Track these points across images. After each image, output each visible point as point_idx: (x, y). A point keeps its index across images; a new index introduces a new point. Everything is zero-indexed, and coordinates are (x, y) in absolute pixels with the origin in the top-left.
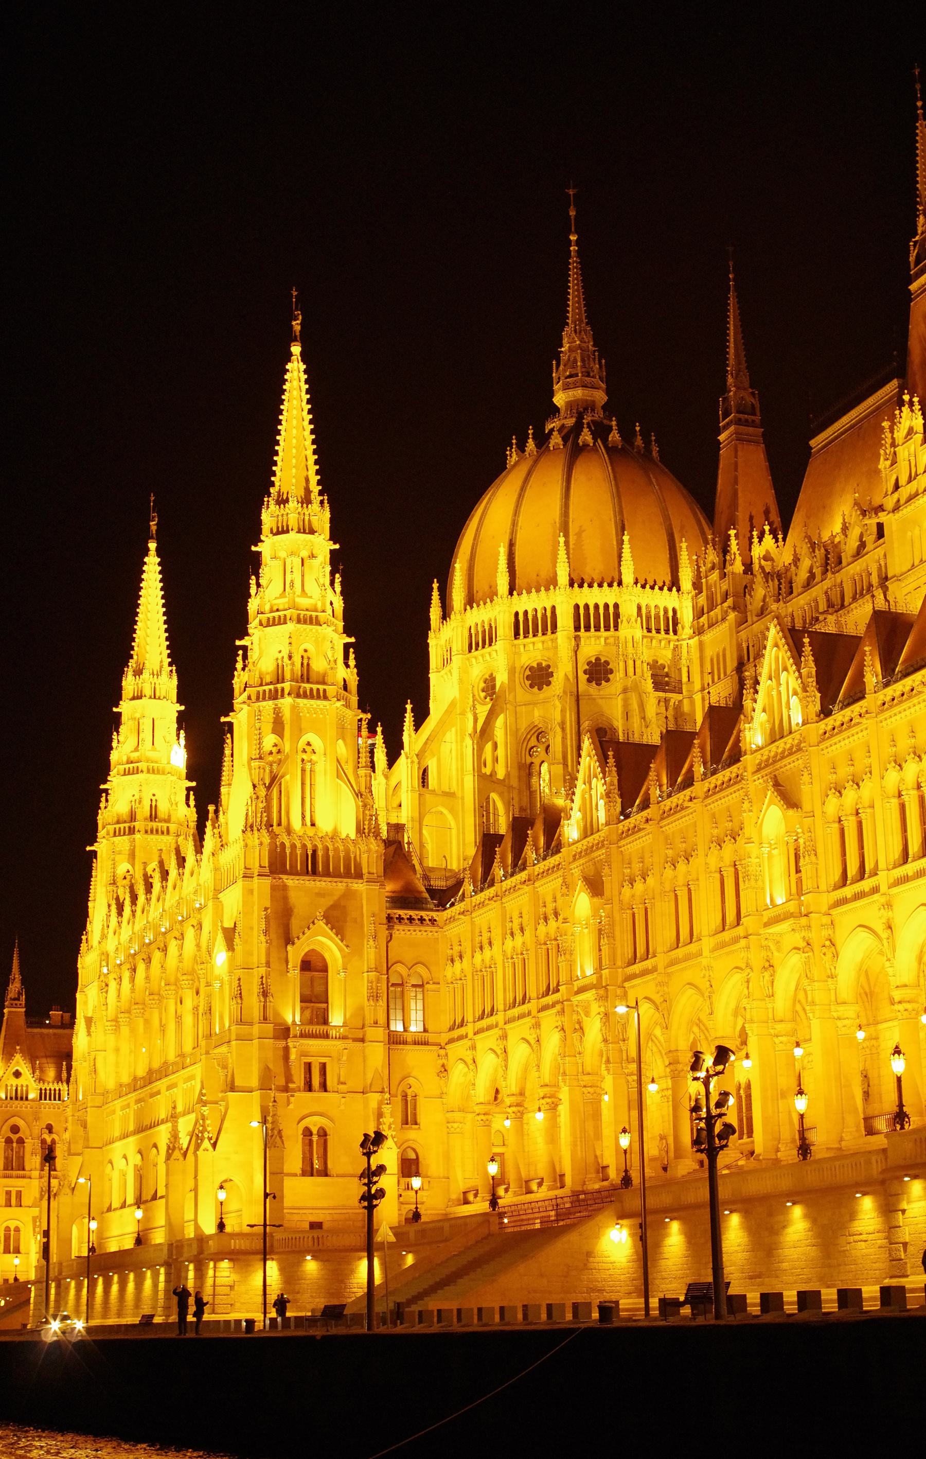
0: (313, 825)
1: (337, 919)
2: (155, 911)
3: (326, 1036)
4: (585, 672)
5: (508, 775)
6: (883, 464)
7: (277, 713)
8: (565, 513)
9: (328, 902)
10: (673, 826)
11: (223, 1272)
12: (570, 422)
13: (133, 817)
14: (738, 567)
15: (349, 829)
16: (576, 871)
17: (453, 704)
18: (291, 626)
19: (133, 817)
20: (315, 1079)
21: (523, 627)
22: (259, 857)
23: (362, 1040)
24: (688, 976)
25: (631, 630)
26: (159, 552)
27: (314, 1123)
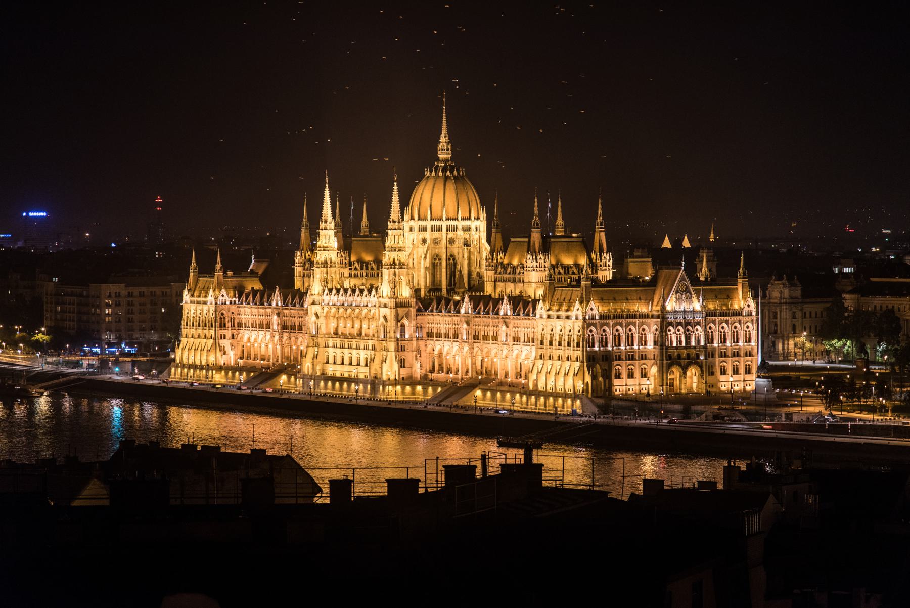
1: (407, 315)
10: (485, 320)
11: (389, 388)
19: (326, 262)
21: (435, 229)
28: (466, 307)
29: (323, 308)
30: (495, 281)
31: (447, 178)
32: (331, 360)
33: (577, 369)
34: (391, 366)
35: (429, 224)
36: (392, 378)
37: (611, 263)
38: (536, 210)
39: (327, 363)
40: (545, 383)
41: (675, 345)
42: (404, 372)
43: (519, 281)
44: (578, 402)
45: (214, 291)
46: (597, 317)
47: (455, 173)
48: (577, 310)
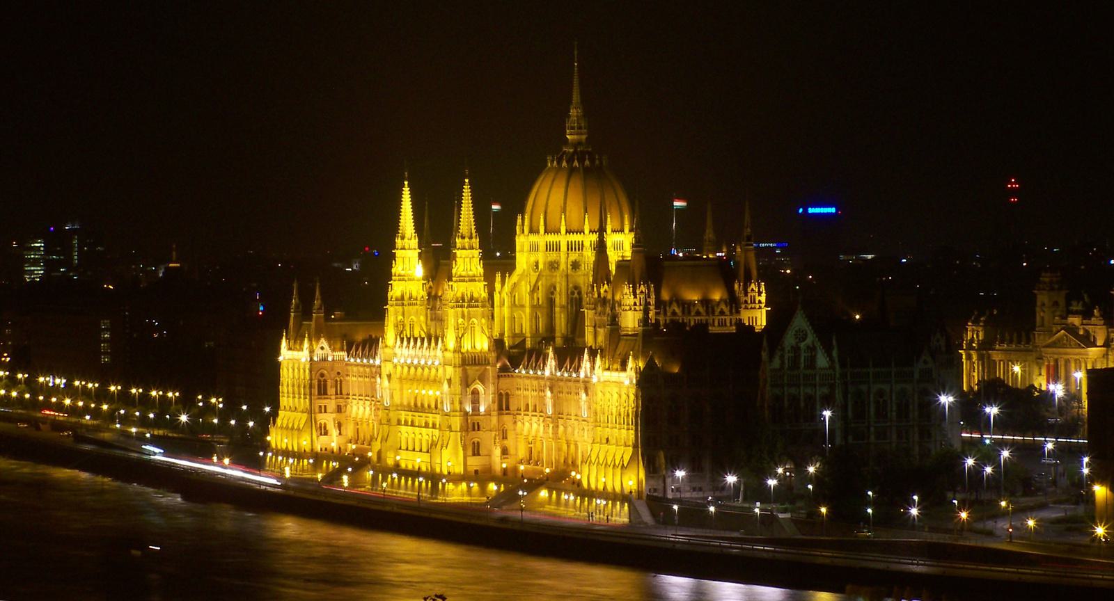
0: (474, 347)
1: (482, 379)
3: (479, 415)
4: (571, 265)
5: (543, 303)
7: (463, 312)
8: (565, 203)
9: (479, 373)
11: (450, 486)
13: (402, 298)
14: (596, 296)
15: (486, 348)
16: (548, 383)
19: (402, 298)
20: (476, 427)
22: (458, 361)
23: (490, 415)
26: (409, 186)
27: (476, 440)
29: (395, 366)
31: (572, 171)
32: (404, 447)
37: (763, 298)
39: (400, 449)
42: (475, 463)
45: (310, 340)
47: (587, 163)
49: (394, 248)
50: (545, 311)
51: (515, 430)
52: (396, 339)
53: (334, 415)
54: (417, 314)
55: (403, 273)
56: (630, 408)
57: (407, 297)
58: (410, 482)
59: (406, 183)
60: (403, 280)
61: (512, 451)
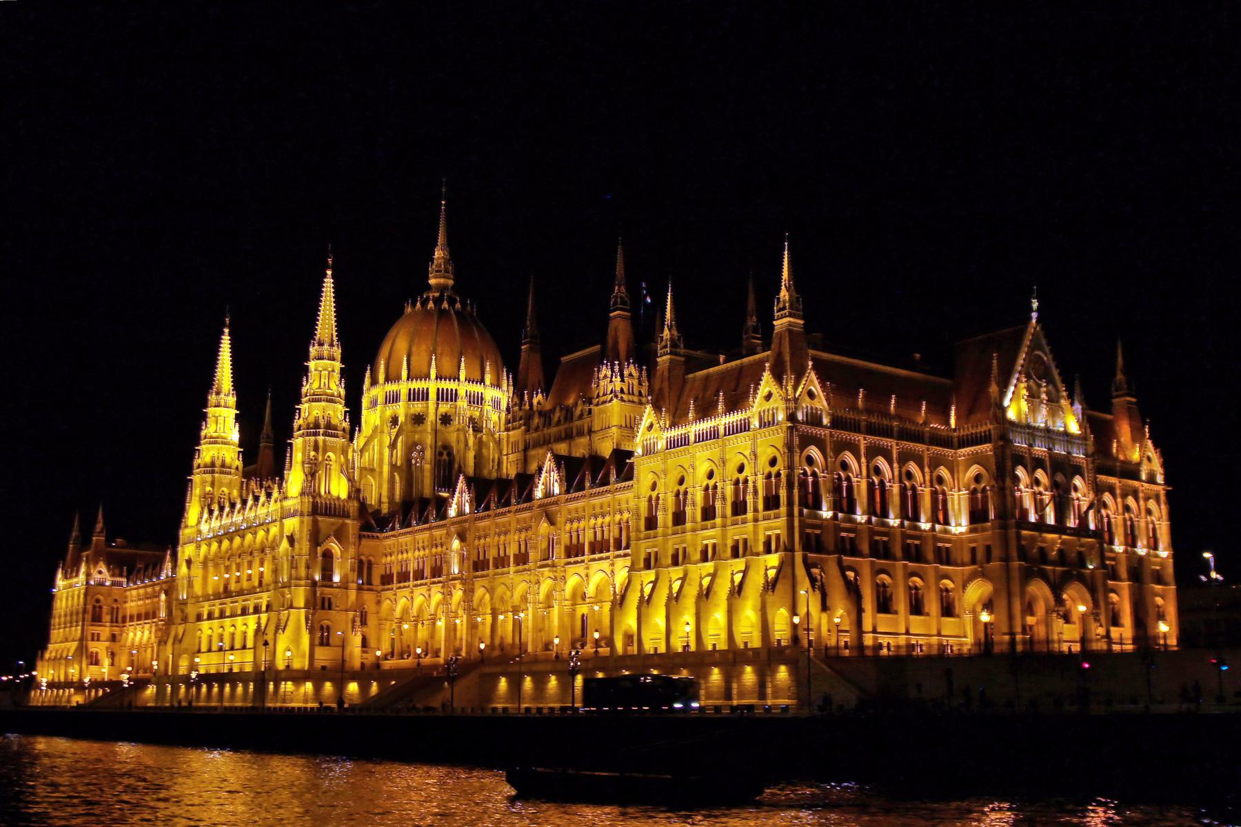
1: (340, 535)
2: (237, 518)
6: (594, 386)
7: (316, 442)
9: (335, 528)
10: (500, 520)
11: (288, 686)
12: (437, 295)
14: (527, 407)
15: (344, 495)
16: (453, 529)
17: (376, 427)
18: (324, 404)
19: (213, 464)
20: (327, 604)
22: (307, 508)
23: (347, 588)
24: (502, 580)
25: (462, 403)
26: (230, 334)
28: (460, 501)
30: (526, 449)
32: (204, 648)
33: (772, 573)
34: (297, 640)
35: (403, 387)
36: (297, 665)
38: (620, 270)
39: (199, 651)
40: (660, 631)
41: (1032, 518)
42: (324, 656)
43: (581, 434)
44: (783, 673)
45: (87, 562)
46: (826, 421)
47: (458, 306)
48: (768, 397)
49: (206, 406)
50: (404, 474)
51: (378, 613)
52: (202, 513)
53: (107, 644)
54: (230, 485)
55: (215, 435)
56: (760, 477)
57: (218, 463)
58: (216, 690)
59: (226, 331)
60: (215, 443)
61: (372, 642)
